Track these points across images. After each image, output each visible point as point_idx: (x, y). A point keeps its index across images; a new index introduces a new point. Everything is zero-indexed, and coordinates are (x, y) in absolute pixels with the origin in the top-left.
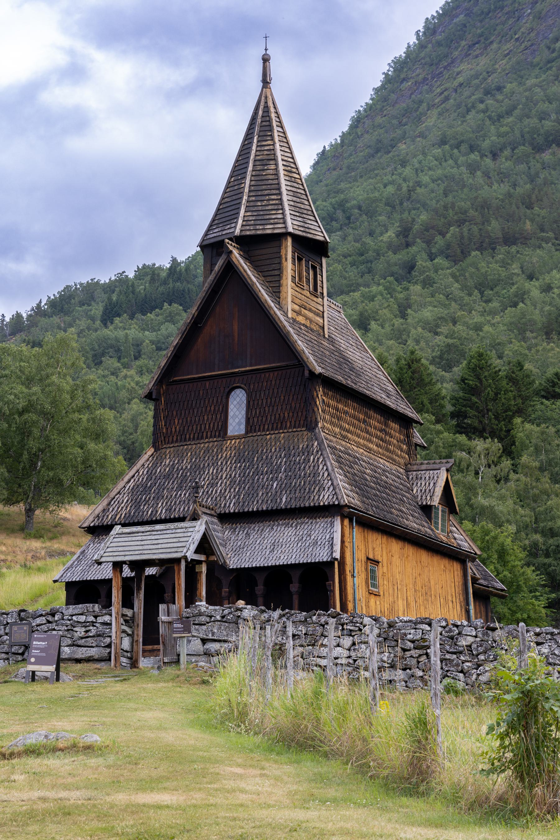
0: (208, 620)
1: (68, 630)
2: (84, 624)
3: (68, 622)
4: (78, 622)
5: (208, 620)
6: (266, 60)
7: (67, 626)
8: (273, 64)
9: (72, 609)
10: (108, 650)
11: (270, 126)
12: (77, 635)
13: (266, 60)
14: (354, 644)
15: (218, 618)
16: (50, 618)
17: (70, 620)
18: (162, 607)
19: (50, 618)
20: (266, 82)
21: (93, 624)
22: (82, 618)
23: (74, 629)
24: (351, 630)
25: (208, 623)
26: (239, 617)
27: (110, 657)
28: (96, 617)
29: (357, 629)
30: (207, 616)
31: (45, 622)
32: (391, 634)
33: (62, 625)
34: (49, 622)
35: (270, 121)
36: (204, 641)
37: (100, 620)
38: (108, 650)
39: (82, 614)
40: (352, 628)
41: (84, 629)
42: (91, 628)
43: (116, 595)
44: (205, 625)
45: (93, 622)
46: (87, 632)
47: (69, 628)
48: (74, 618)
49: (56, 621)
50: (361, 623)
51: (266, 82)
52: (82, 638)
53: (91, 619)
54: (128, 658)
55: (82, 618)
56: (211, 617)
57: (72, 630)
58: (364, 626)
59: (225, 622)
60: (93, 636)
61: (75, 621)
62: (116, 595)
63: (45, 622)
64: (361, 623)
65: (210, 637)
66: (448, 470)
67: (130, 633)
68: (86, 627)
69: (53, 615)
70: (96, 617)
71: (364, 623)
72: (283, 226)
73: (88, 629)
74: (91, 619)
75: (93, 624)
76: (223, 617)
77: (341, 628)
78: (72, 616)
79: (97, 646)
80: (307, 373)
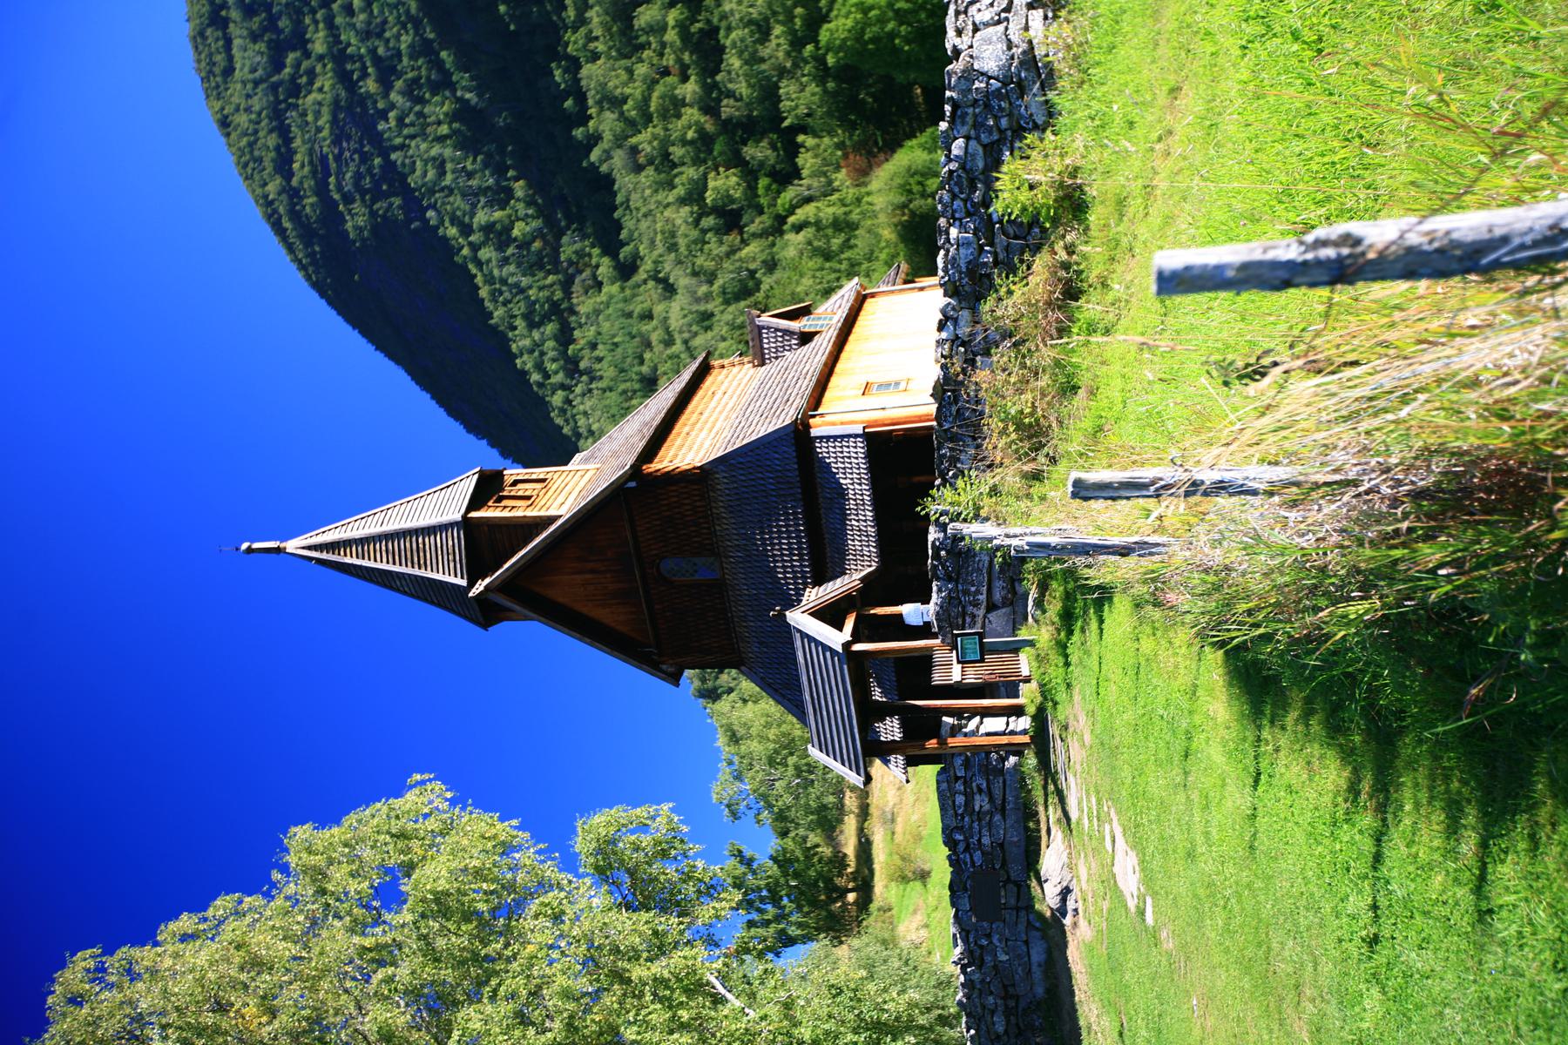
1: (980, 820)
12: (987, 807)
19: (961, 847)
22: (960, 799)
23: (977, 808)
28: (957, 779)
33: (971, 827)
36: (992, 607)
41: (977, 797)
44: (964, 608)
45: (965, 783)
46: (980, 790)
52: (991, 800)
70: (957, 779)
74: (960, 786)
80: (632, 484)
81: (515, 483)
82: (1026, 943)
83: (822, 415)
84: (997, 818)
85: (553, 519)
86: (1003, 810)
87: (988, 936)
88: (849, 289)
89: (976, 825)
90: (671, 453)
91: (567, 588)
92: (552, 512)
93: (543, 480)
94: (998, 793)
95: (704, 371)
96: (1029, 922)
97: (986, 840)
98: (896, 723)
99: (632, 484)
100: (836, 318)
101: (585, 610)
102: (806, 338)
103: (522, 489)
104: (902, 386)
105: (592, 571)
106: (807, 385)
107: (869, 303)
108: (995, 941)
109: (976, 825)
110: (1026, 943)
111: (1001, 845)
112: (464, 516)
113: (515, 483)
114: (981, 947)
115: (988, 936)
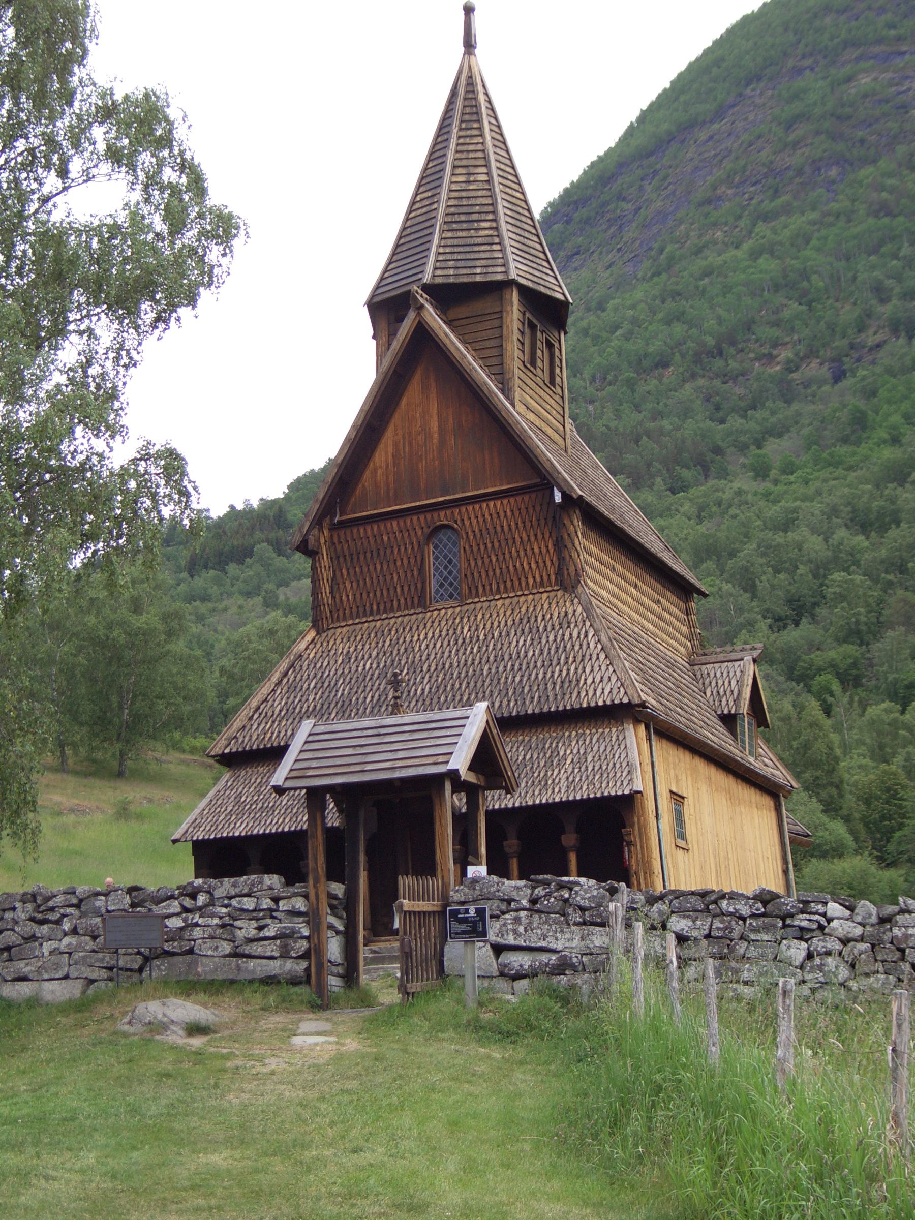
0: (504, 907)
1: (223, 926)
2: (253, 914)
3: (224, 910)
4: (242, 910)
5: (504, 907)
6: (469, 10)
7: (221, 918)
8: (478, 18)
9: (225, 886)
10: (304, 964)
11: (478, 113)
12: (240, 934)
13: (469, 10)
14: (810, 956)
15: (525, 903)
16: (188, 903)
17: (226, 906)
18: (405, 882)
19: (188, 903)
20: (469, 45)
21: (271, 913)
22: (249, 903)
23: (238, 923)
24: (802, 929)
25: (504, 913)
26: (566, 901)
27: (309, 976)
28: (276, 900)
29: (815, 926)
30: (503, 900)
31: (178, 910)
32: (887, 937)
33: (213, 915)
34: (186, 910)
35: (477, 106)
36: (498, 949)
37: (283, 905)
38: (304, 964)
39: (248, 895)
40: (805, 924)
41: (254, 924)
42: (269, 921)
43: (317, 858)
45: (271, 910)
46: (260, 928)
47: (227, 919)
48: (234, 902)
49: (200, 909)
50: (824, 915)
51: (469, 45)
53: (266, 903)
54: (339, 975)
55: (249, 903)
56: (509, 901)
57: (232, 925)
58: (829, 921)
59: (538, 911)
60: (274, 938)
61: (235, 909)
62: (317, 858)
63: (178, 910)
64: (824, 915)
65: (511, 940)
66: (755, 661)
67: (341, 928)
68: (257, 920)
69: (193, 896)
70: (276, 900)
71: (829, 914)
72: (503, 269)
73: (262, 923)
74: (266, 903)
75: (271, 913)
76: (534, 901)
77: (780, 925)
78: (230, 898)
79: (281, 956)
80: (558, 497)
81: (550, 346)
82: (66, 977)
83: (649, 739)
84: (227, 948)
85: (507, 391)
86: (235, 955)
87: (74, 931)
88: (780, 774)
89: (216, 921)
90: (593, 548)
91: (423, 407)
92: (518, 394)
93: (552, 381)
94: (257, 949)
95: (683, 589)
96: (92, 981)
97: (197, 933)
98: (336, 824)
99: (558, 497)
100: (752, 760)
101: (390, 433)
102: (729, 721)
103: (542, 353)
104: (681, 843)
105: (442, 441)
106: (679, 720)
107: (767, 801)
108: (66, 940)
109: (216, 921)
110: (66, 977)
111: (191, 951)
112: (512, 283)
113: (550, 346)
114: (58, 922)
115: (74, 931)
